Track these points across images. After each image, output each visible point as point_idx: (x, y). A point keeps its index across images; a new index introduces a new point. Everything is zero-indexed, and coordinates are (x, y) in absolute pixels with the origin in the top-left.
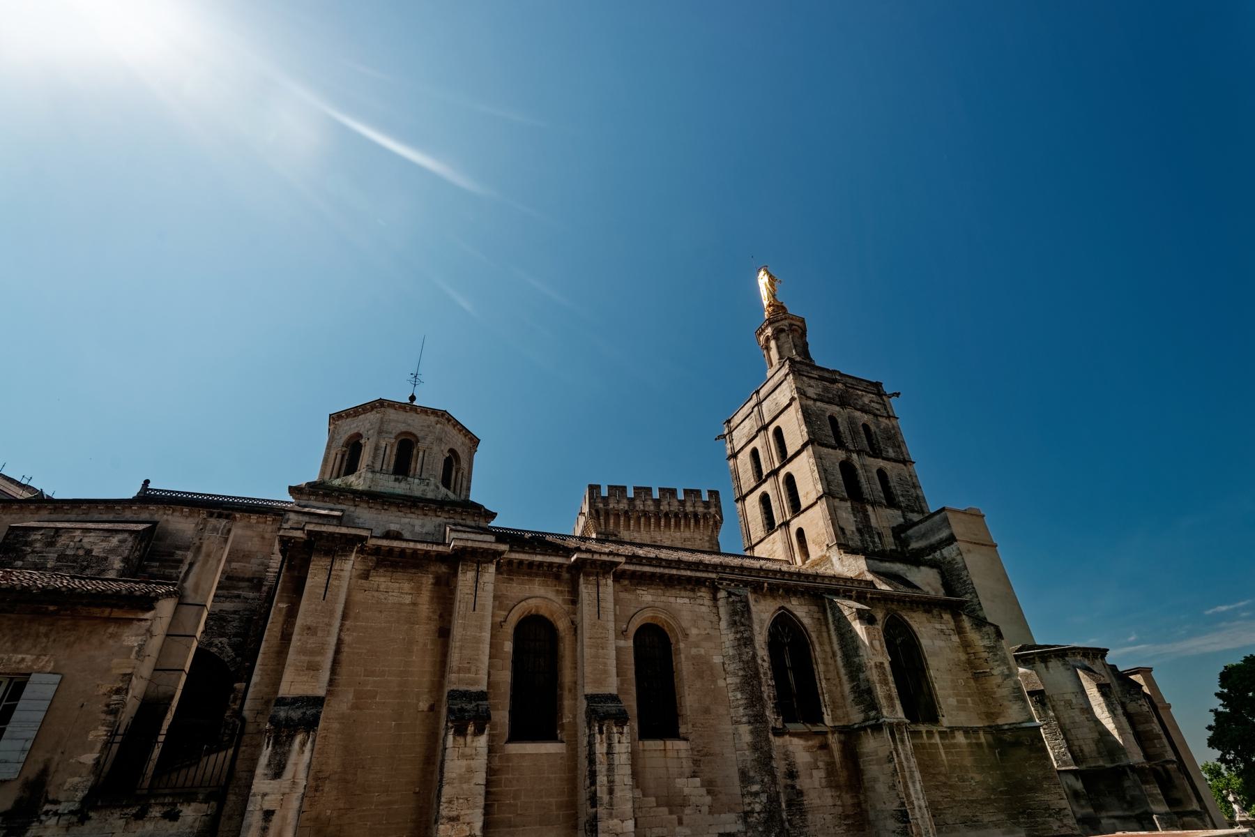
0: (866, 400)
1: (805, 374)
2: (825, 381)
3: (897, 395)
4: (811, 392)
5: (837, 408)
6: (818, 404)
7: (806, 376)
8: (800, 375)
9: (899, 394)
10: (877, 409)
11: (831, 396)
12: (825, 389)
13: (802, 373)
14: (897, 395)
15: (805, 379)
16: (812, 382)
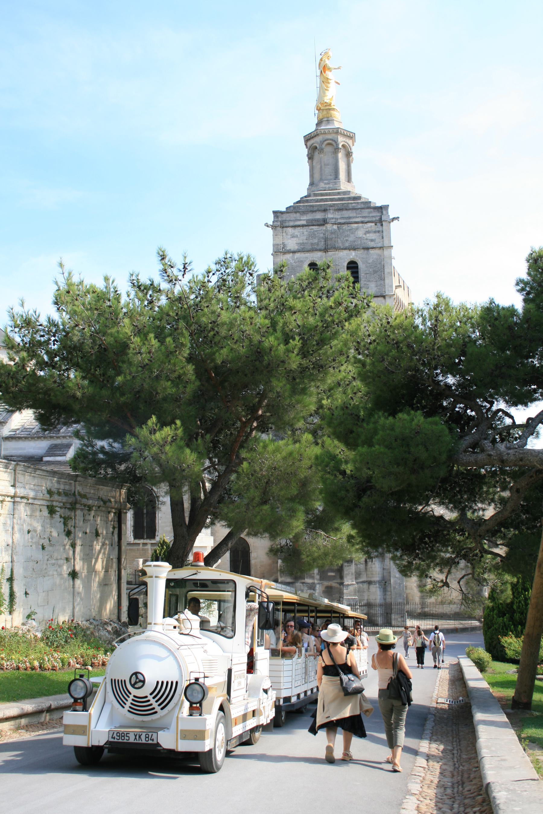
0: (360, 233)
1: (291, 224)
2: (313, 225)
3: (397, 218)
4: (292, 244)
5: (319, 254)
6: (297, 255)
7: (292, 227)
8: (283, 227)
9: (398, 218)
10: (372, 240)
11: (316, 241)
12: (312, 235)
13: (287, 224)
14: (397, 218)
15: (290, 230)
16: (297, 231)
